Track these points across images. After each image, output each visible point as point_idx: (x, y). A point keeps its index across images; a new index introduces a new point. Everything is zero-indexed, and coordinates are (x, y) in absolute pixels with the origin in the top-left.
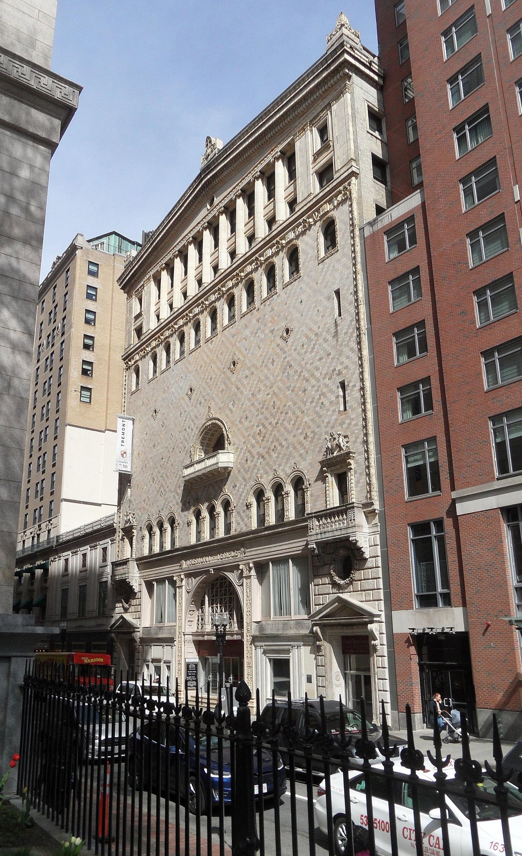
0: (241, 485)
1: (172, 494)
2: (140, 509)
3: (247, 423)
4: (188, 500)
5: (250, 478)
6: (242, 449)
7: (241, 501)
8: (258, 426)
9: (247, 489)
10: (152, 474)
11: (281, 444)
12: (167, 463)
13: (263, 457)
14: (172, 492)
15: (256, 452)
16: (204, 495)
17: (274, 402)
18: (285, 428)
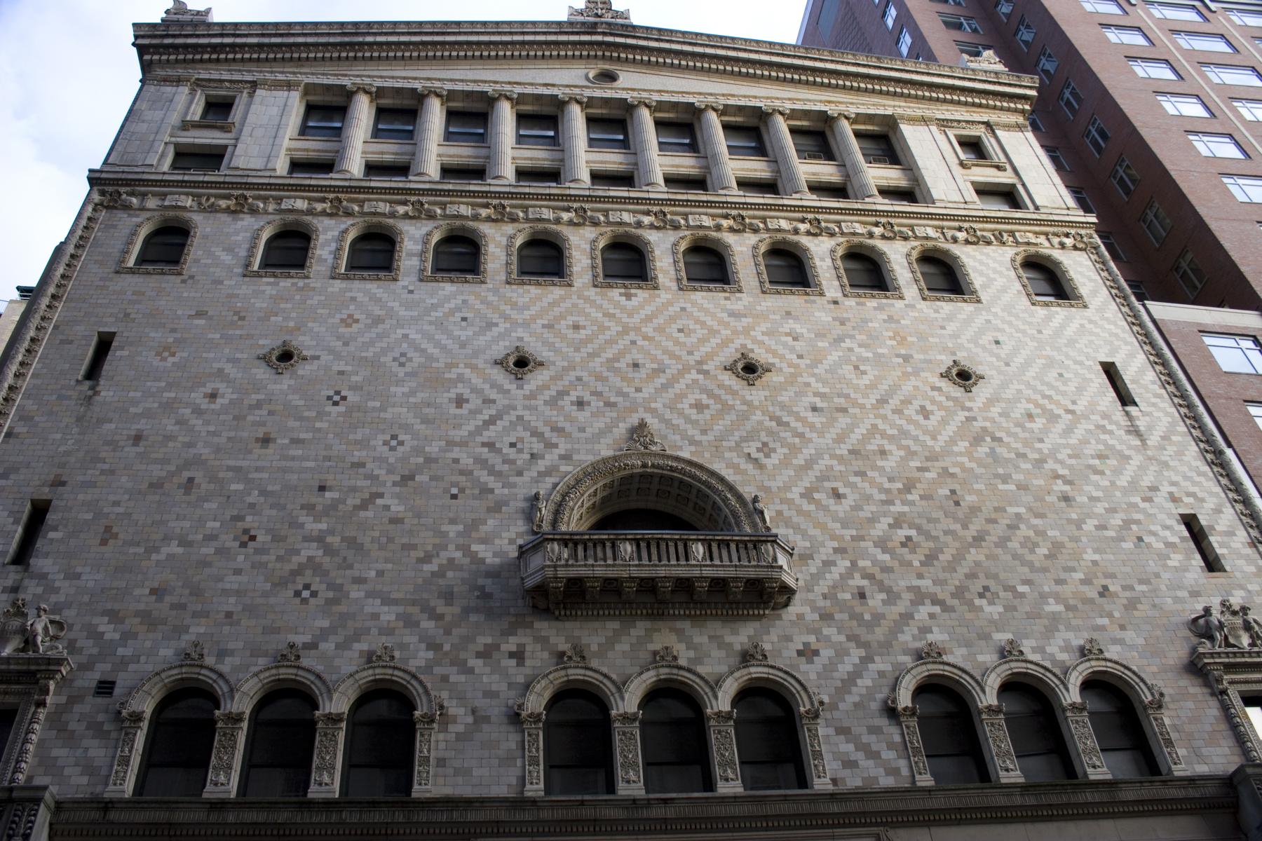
0: (841, 653)
1: (400, 609)
2: (114, 616)
3: (842, 508)
4: (514, 649)
5: (886, 646)
6: (828, 564)
7: (851, 699)
8: (897, 524)
9: (881, 674)
10: (239, 518)
11: (1012, 589)
12: (364, 506)
13: (935, 602)
14: (387, 601)
15: (903, 583)
16: (623, 646)
17: (953, 492)
18: (1015, 556)
